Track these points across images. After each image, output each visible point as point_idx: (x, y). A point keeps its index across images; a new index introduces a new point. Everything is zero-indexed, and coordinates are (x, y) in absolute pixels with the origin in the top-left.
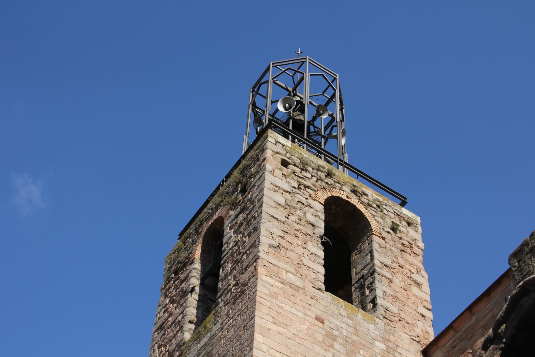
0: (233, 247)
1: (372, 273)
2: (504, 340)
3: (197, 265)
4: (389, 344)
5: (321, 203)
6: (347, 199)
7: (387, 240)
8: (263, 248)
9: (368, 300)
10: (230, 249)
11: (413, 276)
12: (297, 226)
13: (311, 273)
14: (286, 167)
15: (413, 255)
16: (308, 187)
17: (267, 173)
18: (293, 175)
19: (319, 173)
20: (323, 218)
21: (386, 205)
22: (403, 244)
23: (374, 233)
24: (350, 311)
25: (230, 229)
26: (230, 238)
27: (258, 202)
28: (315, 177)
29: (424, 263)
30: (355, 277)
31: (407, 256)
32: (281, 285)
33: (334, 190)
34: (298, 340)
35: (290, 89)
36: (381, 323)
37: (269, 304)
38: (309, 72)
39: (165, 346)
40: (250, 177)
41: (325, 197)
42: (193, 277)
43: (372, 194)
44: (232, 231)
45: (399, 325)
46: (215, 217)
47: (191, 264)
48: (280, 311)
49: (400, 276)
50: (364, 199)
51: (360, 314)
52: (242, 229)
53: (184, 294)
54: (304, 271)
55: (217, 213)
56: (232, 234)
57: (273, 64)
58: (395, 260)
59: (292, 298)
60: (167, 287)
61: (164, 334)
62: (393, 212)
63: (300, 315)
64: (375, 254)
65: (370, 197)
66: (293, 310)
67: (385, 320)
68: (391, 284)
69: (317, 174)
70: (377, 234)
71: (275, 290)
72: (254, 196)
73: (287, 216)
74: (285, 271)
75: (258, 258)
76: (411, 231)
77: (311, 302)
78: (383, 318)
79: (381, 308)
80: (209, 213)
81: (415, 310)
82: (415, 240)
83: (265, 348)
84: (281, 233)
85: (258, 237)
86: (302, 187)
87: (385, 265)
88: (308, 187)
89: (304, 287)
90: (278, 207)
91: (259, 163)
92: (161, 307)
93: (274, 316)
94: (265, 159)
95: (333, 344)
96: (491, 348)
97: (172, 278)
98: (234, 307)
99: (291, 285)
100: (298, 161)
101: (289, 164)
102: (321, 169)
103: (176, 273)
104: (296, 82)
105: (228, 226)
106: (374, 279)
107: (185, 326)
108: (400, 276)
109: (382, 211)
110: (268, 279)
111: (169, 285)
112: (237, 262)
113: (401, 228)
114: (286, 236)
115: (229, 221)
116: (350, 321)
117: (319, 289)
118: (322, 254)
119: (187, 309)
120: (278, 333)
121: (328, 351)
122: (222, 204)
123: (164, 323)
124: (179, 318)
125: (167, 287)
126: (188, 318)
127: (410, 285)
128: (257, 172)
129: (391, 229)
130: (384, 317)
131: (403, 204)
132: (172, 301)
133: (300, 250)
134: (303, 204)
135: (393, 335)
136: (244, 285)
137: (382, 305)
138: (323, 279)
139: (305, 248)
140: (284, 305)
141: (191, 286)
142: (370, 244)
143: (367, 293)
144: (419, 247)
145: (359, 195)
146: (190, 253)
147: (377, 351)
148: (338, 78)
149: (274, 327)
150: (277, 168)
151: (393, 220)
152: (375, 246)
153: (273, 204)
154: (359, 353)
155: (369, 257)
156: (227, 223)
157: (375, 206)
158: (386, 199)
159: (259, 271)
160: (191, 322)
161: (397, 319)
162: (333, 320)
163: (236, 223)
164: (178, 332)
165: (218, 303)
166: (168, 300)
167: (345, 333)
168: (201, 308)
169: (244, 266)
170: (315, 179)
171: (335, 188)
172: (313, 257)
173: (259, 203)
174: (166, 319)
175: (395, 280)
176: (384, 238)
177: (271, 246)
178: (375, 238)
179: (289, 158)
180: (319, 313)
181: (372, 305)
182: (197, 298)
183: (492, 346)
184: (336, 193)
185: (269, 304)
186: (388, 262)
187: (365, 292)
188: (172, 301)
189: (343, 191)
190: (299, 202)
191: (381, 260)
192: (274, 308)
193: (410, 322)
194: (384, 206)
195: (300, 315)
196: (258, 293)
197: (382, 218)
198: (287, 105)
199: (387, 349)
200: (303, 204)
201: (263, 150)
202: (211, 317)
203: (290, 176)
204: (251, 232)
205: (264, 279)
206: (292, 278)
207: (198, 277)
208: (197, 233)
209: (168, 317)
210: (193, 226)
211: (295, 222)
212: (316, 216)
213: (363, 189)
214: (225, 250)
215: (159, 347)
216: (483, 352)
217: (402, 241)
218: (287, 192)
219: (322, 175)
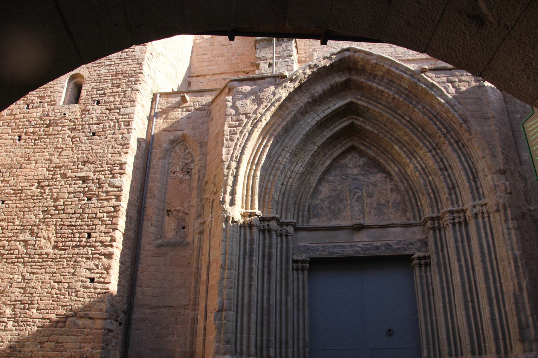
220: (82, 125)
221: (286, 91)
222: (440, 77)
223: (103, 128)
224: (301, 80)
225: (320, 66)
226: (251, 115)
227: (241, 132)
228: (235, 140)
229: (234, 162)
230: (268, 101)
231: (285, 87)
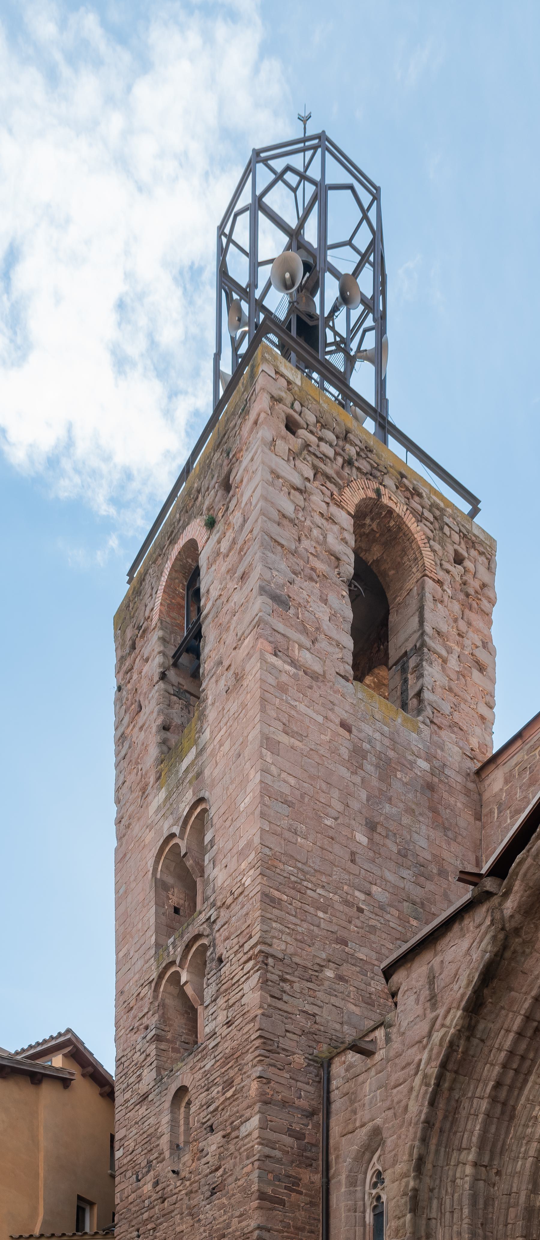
14: (293, 433)
19: (348, 447)
23: (427, 572)
41: (356, 501)
48: (293, 712)
62: (458, 530)
63: (320, 719)
66: (310, 712)
69: (344, 450)
71: (284, 678)
74: (297, 646)
81: (473, 709)
93: (284, 721)
95: (362, 764)
100: (312, 419)
101: (299, 426)
109: (441, 529)
120: (292, 748)
121: (356, 773)
140: (297, 703)
147: (419, 773)
149: (284, 739)
151: (456, 547)
154: (396, 777)
170: (340, 460)
180: (345, 716)
189: (384, 486)
192: (284, 708)
195: (320, 719)
205: (269, 660)
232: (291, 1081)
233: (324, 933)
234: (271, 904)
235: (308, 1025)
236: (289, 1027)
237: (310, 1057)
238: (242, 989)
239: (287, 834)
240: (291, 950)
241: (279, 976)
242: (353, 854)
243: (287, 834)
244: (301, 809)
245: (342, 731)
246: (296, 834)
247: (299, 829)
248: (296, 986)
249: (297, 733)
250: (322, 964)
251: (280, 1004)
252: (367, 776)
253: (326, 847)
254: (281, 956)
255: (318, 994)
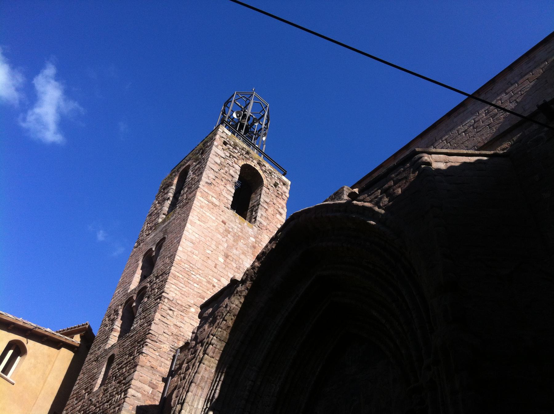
0: (190, 180)
1: (259, 204)
2: (279, 240)
3: (174, 187)
4: (258, 240)
5: (240, 167)
6: (254, 166)
7: (270, 190)
8: (202, 183)
9: (253, 217)
10: (189, 181)
11: (279, 209)
12: (223, 175)
13: (225, 199)
15: (282, 199)
16: (235, 157)
17: (214, 146)
18: (228, 150)
19: (242, 151)
20: (239, 174)
21: (274, 173)
22: (278, 193)
24: (241, 221)
25: (191, 172)
26: (190, 176)
27: (206, 160)
28: (239, 152)
29: (287, 204)
30: (250, 205)
31: (279, 199)
32: (207, 203)
33: (248, 161)
34: (209, 230)
35: (243, 107)
36: (256, 229)
37: (198, 211)
38: (253, 100)
39: (150, 224)
40: (206, 147)
41: (243, 164)
42: (170, 192)
43: (268, 166)
44: (192, 172)
45: (265, 231)
46: (187, 164)
47: (171, 186)
48: (204, 215)
49: (272, 208)
50: (264, 168)
51: (246, 223)
52: (196, 172)
53: (165, 200)
54: (222, 198)
55: (188, 163)
56: (192, 174)
57: (236, 93)
58: (272, 200)
59: (212, 210)
60: (159, 196)
61: (151, 218)
63: (214, 219)
64: (262, 196)
65: (267, 168)
66: (211, 216)
67: (258, 228)
68: (266, 211)
69: (241, 151)
70: (266, 186)
71: (203, 204)
72: (205, 157)
73: (220, 170)
74: (211, 196)
75: (198, 188)
76: (284, 188)
77: (221, 213)
78: (257, 227)
79: (258, 222)
80: (185, 162)
82: (285, 192)
83: (190, 231)
84: (214, 177)
85: (201, 177)
86: (231, 157)
87: (266, 202)
88: (235, 157)
89: (220, 205)
90: (216, 164)
91: (212, 141)
92: (153, 205)
93: (199, 217)
94: (215, 139)
95: (227, 235)
96: (272, 243)
97: (162, 191)
98: (182, 209)
99: (212, 203)
102: (244, 149)
103: (164, 189)
104: (247, 104)
105: (191, 170)
106: (258, 208)
107: (160, 215)
108: (272, 208)
110: (201, 199)
111: (159, 195)
112: (189, 188)
113: (279, 186)
114: (216, 179)
115: (192, 167)
116: (240, 226)
117: (228, 208)
118: (233, 191)
119: (164, 208)
120: (200, 225)
121: (224, 238)
122: (191, 158)
123: (152, 212)
124: (159, 211)
125: (159, 196)
126: (163, 212)
127: (276, 213)
128: (210, 145)
129: (274, 185)
130: (258, 227)
131: (284, 175)
132: (159, 203)
133: (222, 187)
134: (230, 165)
135: (261, 236)
136: (189, 199)
137: (259, 221)
138: (231, 203)
139: (225, 187)
140: (206, 212)
141: (168, 197)
142: (261, 191)
143: (254, 214)
144: (286, 196)
145: (261, 166)
146: (172, 181)
148: (268, 106)
149: (198, 222)
150: (220, 145)
152: (263, 192)
153: (213, 162)
155: (259, 197)
156: (191, 168)
157: (268, 172)
158: (275, 170)
159: (197, 194)
160: (164, 214)
161: (265, 228)
162: (231, 224)
163: (195, 169)
164: (157, 218)
165: (177, 207)
166: (157, 202)
167: (235, 231)
168: (171, 208)
169: (192, 190)
170: (239, 154)
171: (249, 160)
172: (228, 192)
173: (207, 161)
174: (154, 211)
175: (270, 210)
176: (269, 189)
177: (207, 183)
178: (264, 188)
179: (228, 141)
180: (224, 219)
181: (254, 220)
182: (170, 203)
183: (273, 242)
184: (249, 163)
185: (198, 211)
186: (268, 201)
187: (253, 213)
188: (159, 203)
189: (253, 162)
190: (228, 163)
191: (264, 199)
192: (200, 213)
193: (271, 231)
194: (273, 173)
195: (214, 219)
196: (194, 204)
197: (270, 179)
198: (238, 115)
199: (256, 241)
200: (230, 165)
201: (215, 135)
202: (172, 213)
203: (226, 150)
204: (199, 175)
206: (214, 200)
207: (173, 193)
208: (178, 171)
209: (155, 210)
210: (177, 168)
211: (223, 173)
212: (235, 172)
213: (264, 163)
214: (187, 181)
215: (147, 224)
216: (269, 244)
217: (278, 192)
218: (223, 158)
219: (244, 153)
220: (99, 407)
221: (239, 297)
222: (373, 193)
223: (110, 405)
224: (251, 277)
225: (268, 252)
226: (205, 340)
227: (193, 366)
228: (187, 378)
229: (179, 404)
230: (220, 317)
231: (237, 293)
232: (158, 357)
233: (196, 293)
234: (174, 278)
235: (175, 331)
236: (166, 331)
237: (172, 347)
238: (151, 311)
239: (189, 253)
240: (177, 297)
241: (168, 307)
242: (216, 264)
243: (189, 253)
244: (198, 246)
245: (222, 223)
246: (193, 254)
247: (195, 252)
248: (175, 313)
249: (203, 221)
250: (190, 305)
251: (164, 320)
252: (229, 239)
253: (205, 260)
254: (171, 299)
255: (185, 318)
